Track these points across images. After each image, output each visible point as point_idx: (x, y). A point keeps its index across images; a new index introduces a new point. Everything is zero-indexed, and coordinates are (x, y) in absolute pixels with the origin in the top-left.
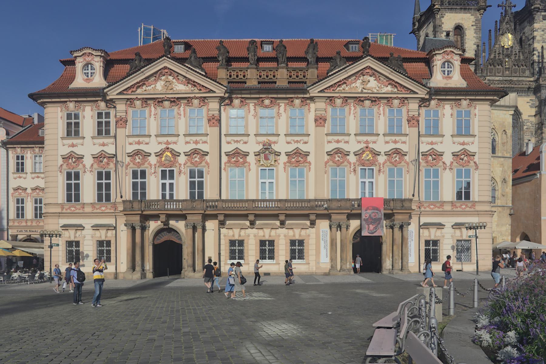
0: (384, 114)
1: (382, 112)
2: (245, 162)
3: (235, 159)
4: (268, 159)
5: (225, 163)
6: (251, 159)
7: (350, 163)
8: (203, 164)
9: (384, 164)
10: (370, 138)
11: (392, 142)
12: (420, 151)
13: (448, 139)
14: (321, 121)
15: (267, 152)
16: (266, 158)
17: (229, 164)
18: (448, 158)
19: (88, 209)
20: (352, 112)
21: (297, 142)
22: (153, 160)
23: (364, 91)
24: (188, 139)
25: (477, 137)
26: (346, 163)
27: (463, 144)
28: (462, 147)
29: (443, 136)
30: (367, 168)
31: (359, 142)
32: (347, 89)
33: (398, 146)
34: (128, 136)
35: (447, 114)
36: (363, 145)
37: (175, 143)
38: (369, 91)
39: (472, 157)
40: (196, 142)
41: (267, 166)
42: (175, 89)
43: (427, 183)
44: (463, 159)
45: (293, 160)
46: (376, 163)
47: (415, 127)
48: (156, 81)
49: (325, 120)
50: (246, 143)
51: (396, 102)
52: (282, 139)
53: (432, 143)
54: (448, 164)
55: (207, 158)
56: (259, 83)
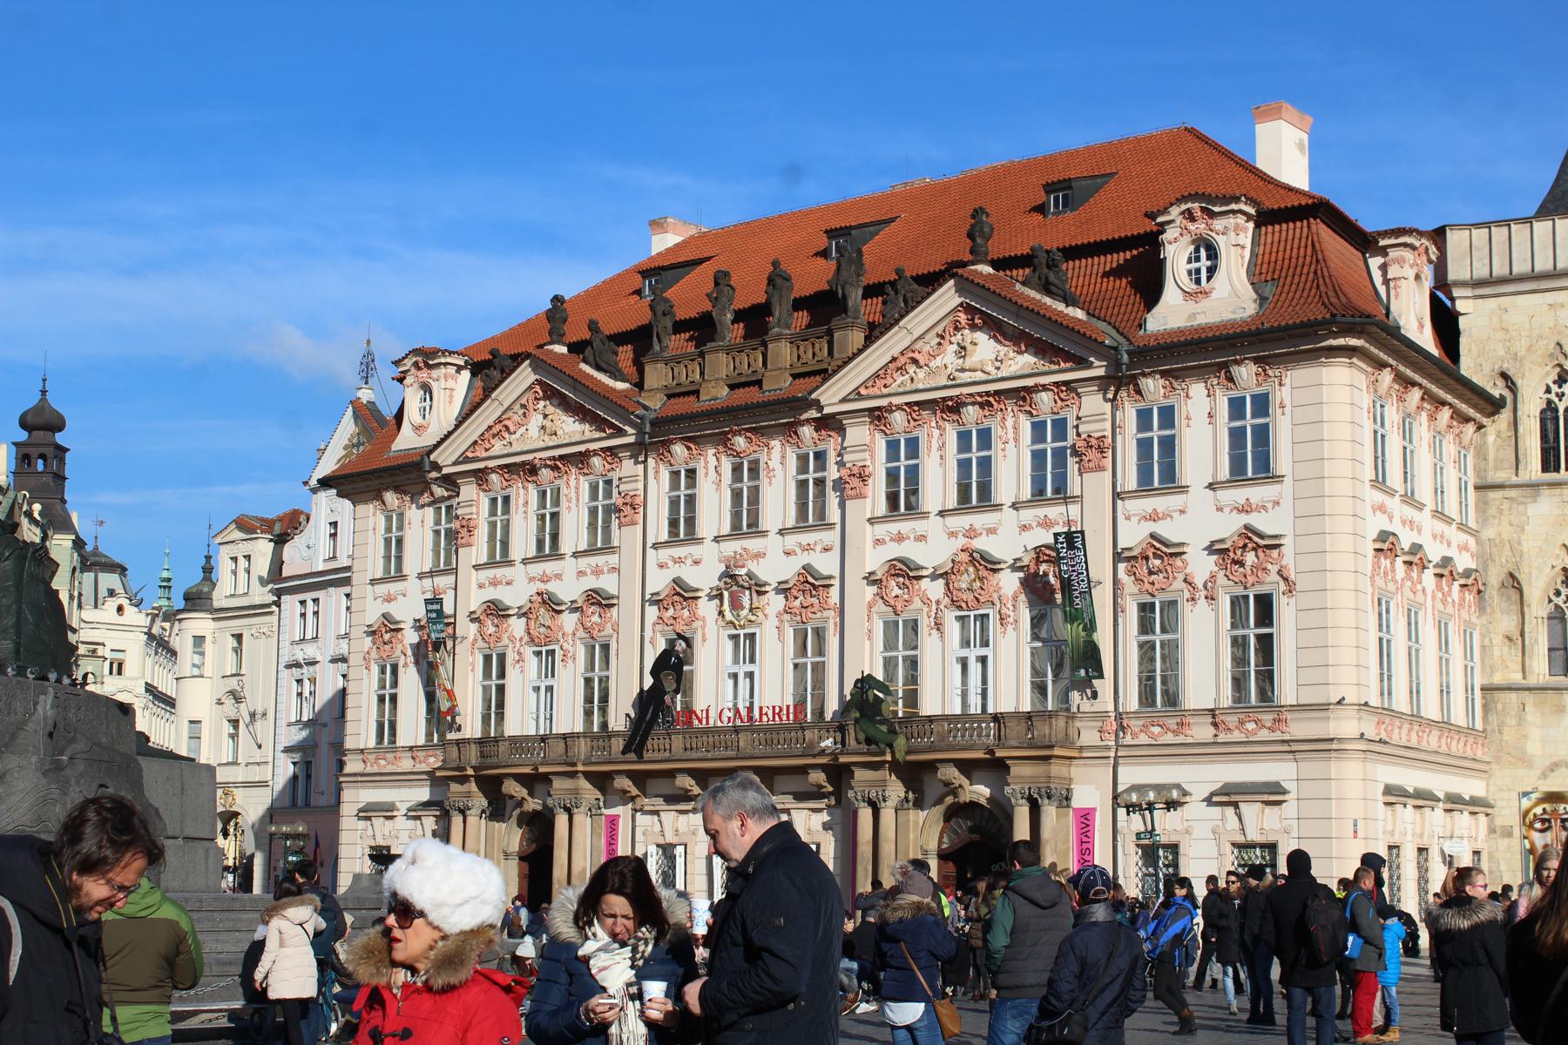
0: (1016, 440)
1: (1011, 435)
2: (694, 617)
3: (671, 612)
4: (742, 608)
5: (654, 624)
6: (707, 608)
7: (926, 601)
8: (608, 630)
9: (1015, 598)
10: (980, 520)
11: (1039, 524)
12: (1121, 545)
13: (1198, 498)
14: (855, 482)
16: (736, 605)
17: (659, 627)
19: (406, 764)
20: (935, 444)
21: (807, 548)
22: (517, 626)
23: (966, 377)
24: (583, 563)
25: (1288, 480)
26: (917, 603)
27: (1245, 509)
29: (1183, 489)
30: (972, 614)
31: (953, 534)
32: (921, 374)
34: (477, 567)
35: (1202, 418)
36: (962, 541)
37: (558, 577)
38: (979, 376)
39: (1275, 553)
40: (597, 572)
41: (743, 627)
42: (560, 432)
44: (1241, 564)
45: (797, 603)
46: (995, 595)
47: (1101, 469)
49: (863, 478)
50: (696, 563)
51: (1045, 398)
52: (772, 544)
53: (1154, 517)
54: (1199, 583)
55: (614, 610)
56: (732, 387)
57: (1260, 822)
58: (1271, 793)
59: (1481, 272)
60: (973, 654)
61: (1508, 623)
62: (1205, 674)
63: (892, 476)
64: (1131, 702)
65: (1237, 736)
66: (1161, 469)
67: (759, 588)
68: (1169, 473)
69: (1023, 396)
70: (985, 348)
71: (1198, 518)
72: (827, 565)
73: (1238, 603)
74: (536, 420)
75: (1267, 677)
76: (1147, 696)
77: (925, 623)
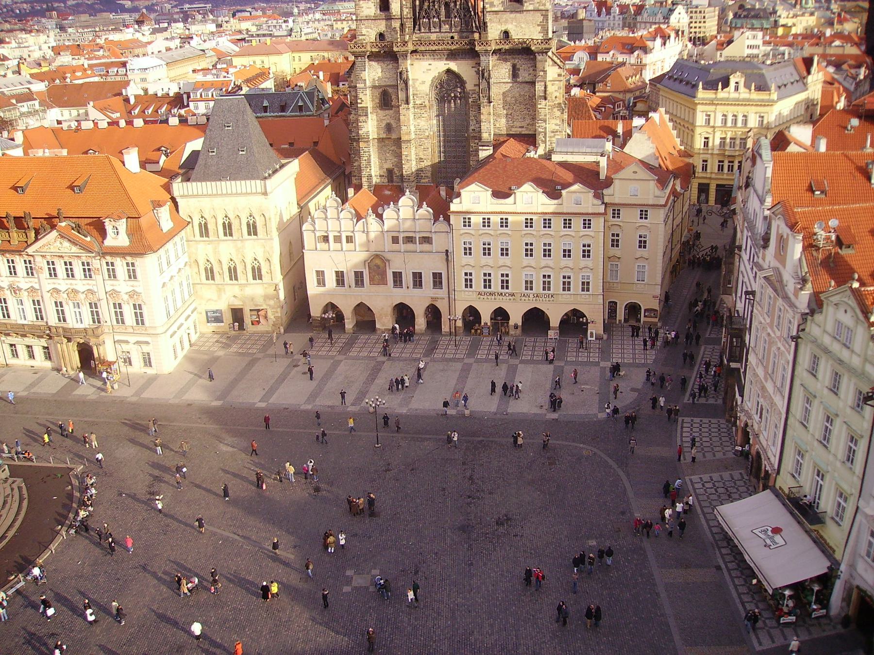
15: (15, 290)
28: (132, 289)
33: (90, 287)
35: (120, 265)
43: (116, 312)
53: (112, 285)
57: (146, 349)
58: (147, 343)
59: (182, 193)
60: (77, 310)
61: (196, 270)
63: (49, 268)
66: (112, 274)
67: (20, 290)
71: (122, 285)
72: (37, 286)
73: (134, 305)
75: (142, 321)
76: (118, 322)
77: (64, 304)
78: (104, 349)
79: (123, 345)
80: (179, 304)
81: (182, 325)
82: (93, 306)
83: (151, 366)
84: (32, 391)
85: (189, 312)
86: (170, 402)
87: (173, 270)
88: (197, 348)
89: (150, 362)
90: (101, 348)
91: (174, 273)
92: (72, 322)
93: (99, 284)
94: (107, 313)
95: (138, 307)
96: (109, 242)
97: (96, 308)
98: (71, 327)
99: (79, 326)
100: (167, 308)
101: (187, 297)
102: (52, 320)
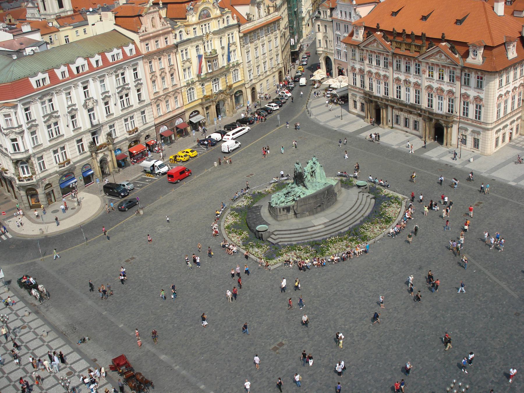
18: (471, 98)
27: (478, 93)
43: (464, 108)
48: (374, 43)
62: (472, 114)
64: (462, 115)
65: (475, 124)
66: (467, 83)
67: (410, 83)
68: (468, 84)
69: (449, 67)
70: (443, 57)
73: (477, 106)
74: (375, 44)
76: (464, 115)
77: (433, 96)
78: (451, 131)
79: (463, 131)
80: (509, 110)
81: (506, 126)
82: (451, 100)
83: (478, 148)
84: (401, 147)
85: (515, 118)
86: (482, 174)
87: (510, 88)
88: (514, 144)
89: (478, 145)
90: (449, 129)
91: (510, 88)
92: (435, 109)
93: (457, 88)
94: (458, 107)
95: (479, 107)
96: (470, 60)
97: (452, 102)
98: (434, 111)
99: (439, 112)
100: (498, 112)
101: (516, 107)
102: (424, 105)
